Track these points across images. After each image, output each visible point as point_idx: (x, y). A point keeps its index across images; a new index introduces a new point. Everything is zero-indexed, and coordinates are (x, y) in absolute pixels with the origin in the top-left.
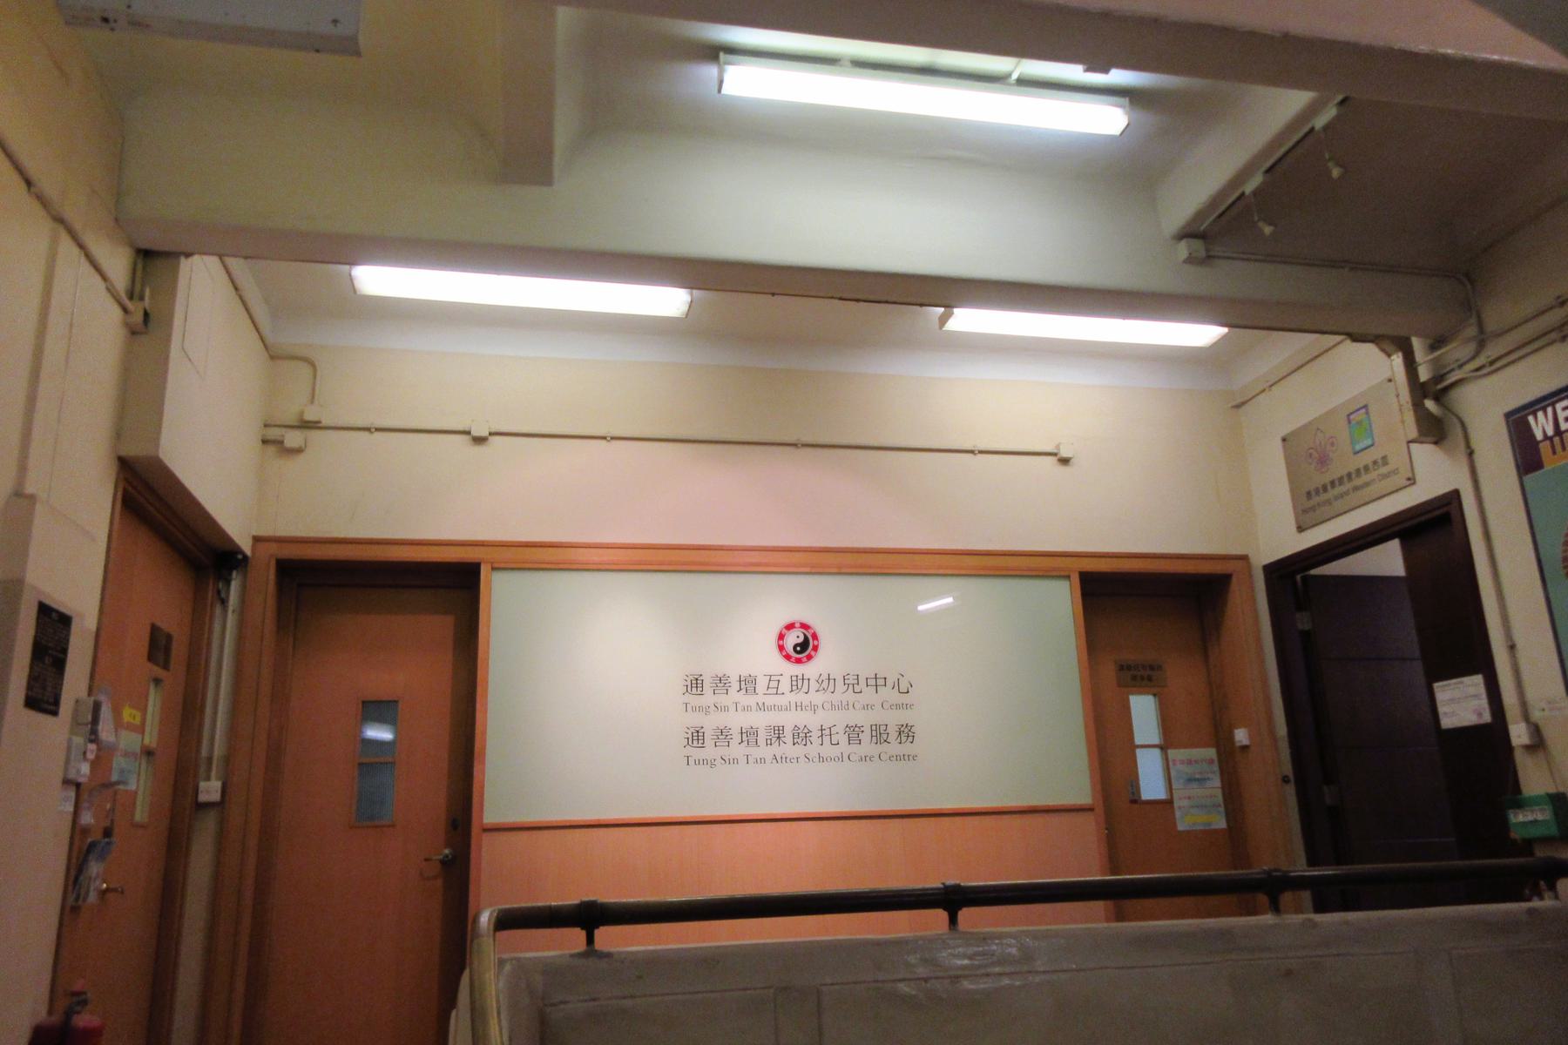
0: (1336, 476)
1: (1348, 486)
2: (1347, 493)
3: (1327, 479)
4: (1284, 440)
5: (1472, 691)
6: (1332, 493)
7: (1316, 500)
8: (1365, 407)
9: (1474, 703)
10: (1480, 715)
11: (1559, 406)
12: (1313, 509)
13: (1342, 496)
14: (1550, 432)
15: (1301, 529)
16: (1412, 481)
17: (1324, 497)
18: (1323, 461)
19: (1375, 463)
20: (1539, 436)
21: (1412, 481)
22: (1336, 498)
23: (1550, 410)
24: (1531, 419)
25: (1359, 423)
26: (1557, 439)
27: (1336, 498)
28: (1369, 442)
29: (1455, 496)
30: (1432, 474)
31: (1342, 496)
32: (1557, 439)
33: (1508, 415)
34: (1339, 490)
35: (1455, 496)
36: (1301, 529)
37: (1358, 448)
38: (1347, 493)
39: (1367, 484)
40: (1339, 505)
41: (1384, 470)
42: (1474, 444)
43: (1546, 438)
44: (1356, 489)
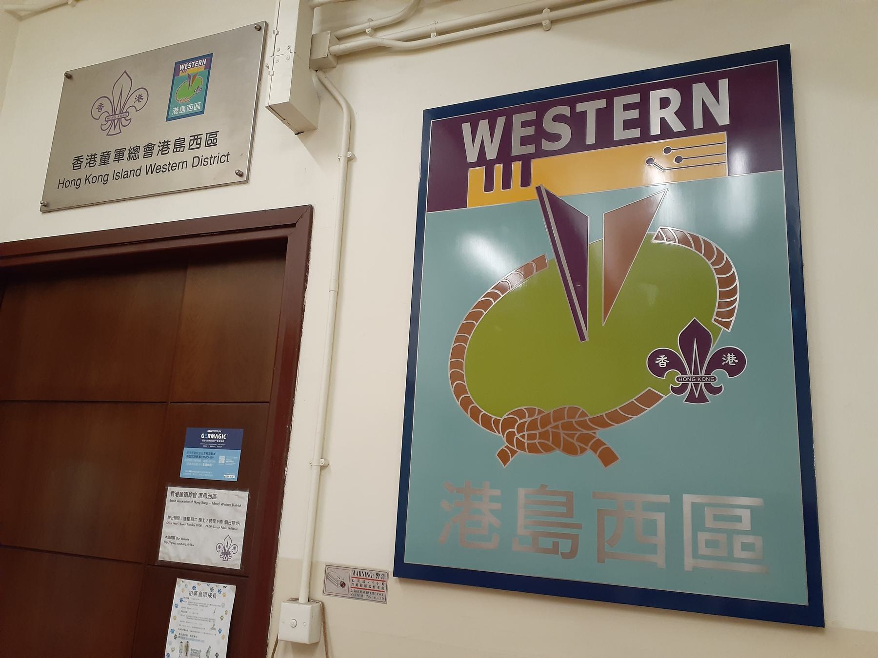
0: (128, 145)
1: (142, 162)
2: (137, 173)
3: (112, 145)
4: (68, 76)
5: (224, 513)
6: (113, 166)
7: (84, 171)
8: (209, 57)
9: (221, 535)
10: (226, 554)
11: (518, 119)
12: (77, 183)
13: (126, 175)
14: (491, 153)
15: (46, 208)
16: (243, 178)
17: (98, 170)
18: (118, 118)
19: (196, 138)
20: (472, 156)
21: (243, 178)
22: (117, 176)
23: (501, 121)
24: (466, 128)
25: (191, 78)
26: (499, 168)
27: (117, 176)
28: (198, 107)
29: (306, 214)
30: (272, 178)
31: (126, 175)
32: (499, 168)
33: (431, 114)
34: (127, 165)
35: (306, 214)
36: (46, 208)
37: (175, 111)
38: (137, 173)
39: (173, 167)
40: (115, 188)
41: (205, 152)
42: (358, 151)
43: (482, 159)
44: (151, 169)
